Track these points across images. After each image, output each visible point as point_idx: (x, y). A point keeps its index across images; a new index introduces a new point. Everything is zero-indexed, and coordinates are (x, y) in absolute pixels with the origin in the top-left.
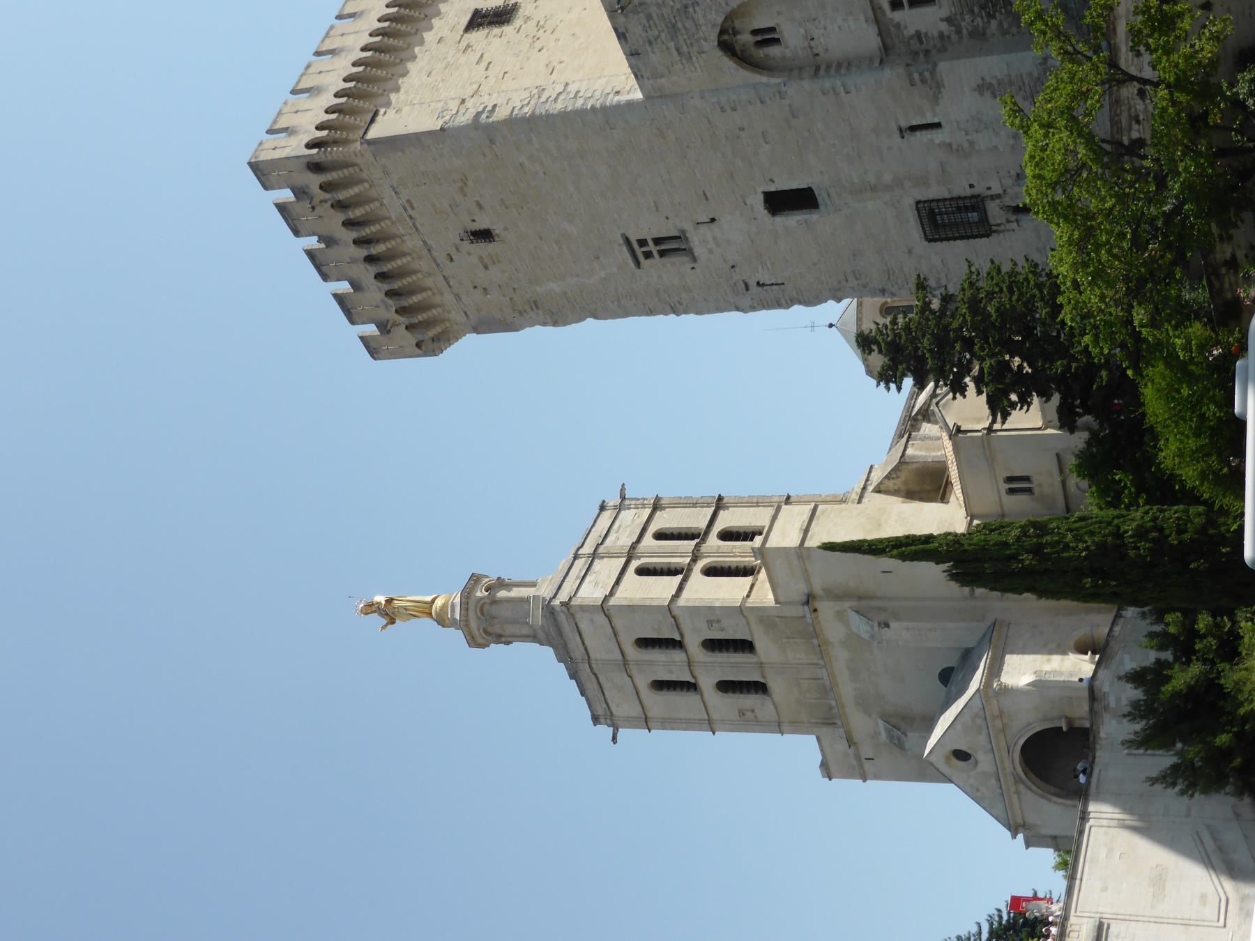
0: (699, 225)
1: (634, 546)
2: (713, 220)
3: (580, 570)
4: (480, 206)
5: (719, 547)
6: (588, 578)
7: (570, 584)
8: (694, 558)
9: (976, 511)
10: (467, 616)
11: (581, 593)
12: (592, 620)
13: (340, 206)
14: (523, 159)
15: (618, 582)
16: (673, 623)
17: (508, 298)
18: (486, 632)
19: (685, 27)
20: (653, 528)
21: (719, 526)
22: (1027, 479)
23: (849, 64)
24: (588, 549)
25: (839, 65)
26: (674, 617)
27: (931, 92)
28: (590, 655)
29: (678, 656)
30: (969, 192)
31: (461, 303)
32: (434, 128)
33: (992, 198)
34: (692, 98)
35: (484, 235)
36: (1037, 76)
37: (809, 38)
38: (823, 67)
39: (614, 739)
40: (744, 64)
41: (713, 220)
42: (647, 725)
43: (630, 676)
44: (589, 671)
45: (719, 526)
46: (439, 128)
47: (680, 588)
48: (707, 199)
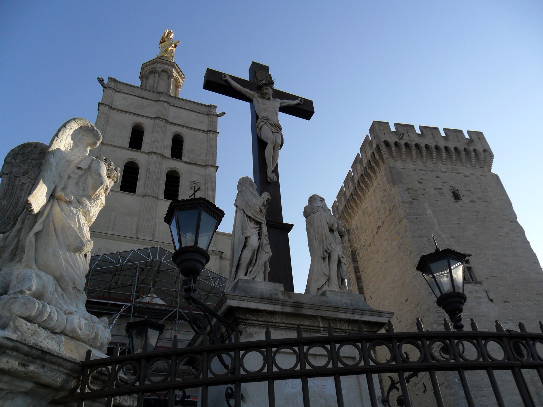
0: (486, 293)
2: (491, 300)
4: (471, 201)
12: (202, 122)
13: (465, 150)
16: (198, 163)
17: (417, 189)
18: (164, 71)
26: (207, 166)
28: (173, 107)
29: (168, 153)
31: (410, 170)
35: (456, 196)
41: (491, 300)
42: (107, 105)
43: (155, 118)
44: (161, 99)
48: (505, 302)
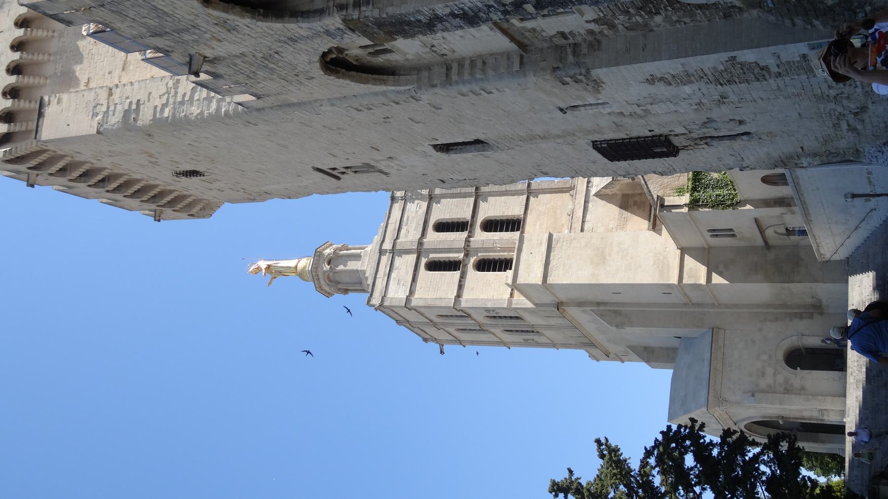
1: (420, 243)
3: (386, 267)
5: (483, 241)
6: (393, 275)
7: (380, 284)
8: (466, 253)
9: (685, 243)
10: (320, 283)
11: (391, 294)
14: (188, 142)
15: (414, 280)
19: (281, 67)
20: (432, 222)
21: (480, 218)
22: (731, 230)
23: (484, 63)
24: (387, 246)
25: (473, 63)
27: (589, 88)
30: (650, 134)
32: (91, 133)
33: (676, 135)
34: (321, 105)
36: (723, 69)
37: (429, 46)
38: (455, 67)
39: (442, 352)
40: (364, 75)
45: (481, 218)
46: (95, 132)
47: (461, 287)
